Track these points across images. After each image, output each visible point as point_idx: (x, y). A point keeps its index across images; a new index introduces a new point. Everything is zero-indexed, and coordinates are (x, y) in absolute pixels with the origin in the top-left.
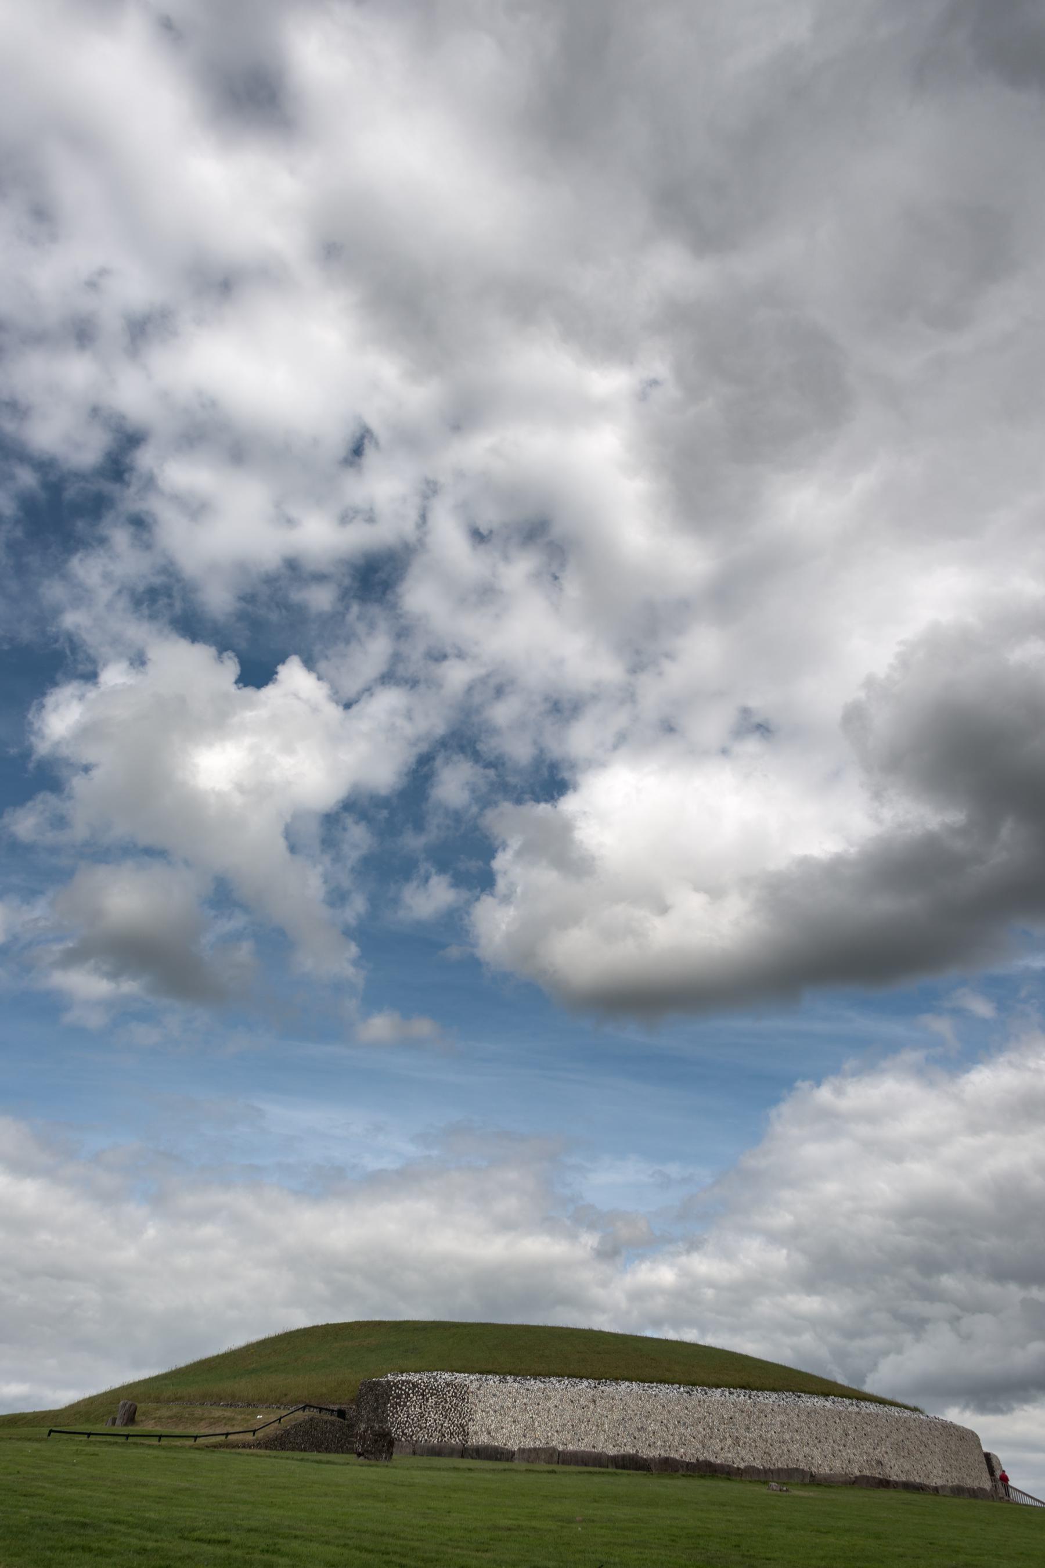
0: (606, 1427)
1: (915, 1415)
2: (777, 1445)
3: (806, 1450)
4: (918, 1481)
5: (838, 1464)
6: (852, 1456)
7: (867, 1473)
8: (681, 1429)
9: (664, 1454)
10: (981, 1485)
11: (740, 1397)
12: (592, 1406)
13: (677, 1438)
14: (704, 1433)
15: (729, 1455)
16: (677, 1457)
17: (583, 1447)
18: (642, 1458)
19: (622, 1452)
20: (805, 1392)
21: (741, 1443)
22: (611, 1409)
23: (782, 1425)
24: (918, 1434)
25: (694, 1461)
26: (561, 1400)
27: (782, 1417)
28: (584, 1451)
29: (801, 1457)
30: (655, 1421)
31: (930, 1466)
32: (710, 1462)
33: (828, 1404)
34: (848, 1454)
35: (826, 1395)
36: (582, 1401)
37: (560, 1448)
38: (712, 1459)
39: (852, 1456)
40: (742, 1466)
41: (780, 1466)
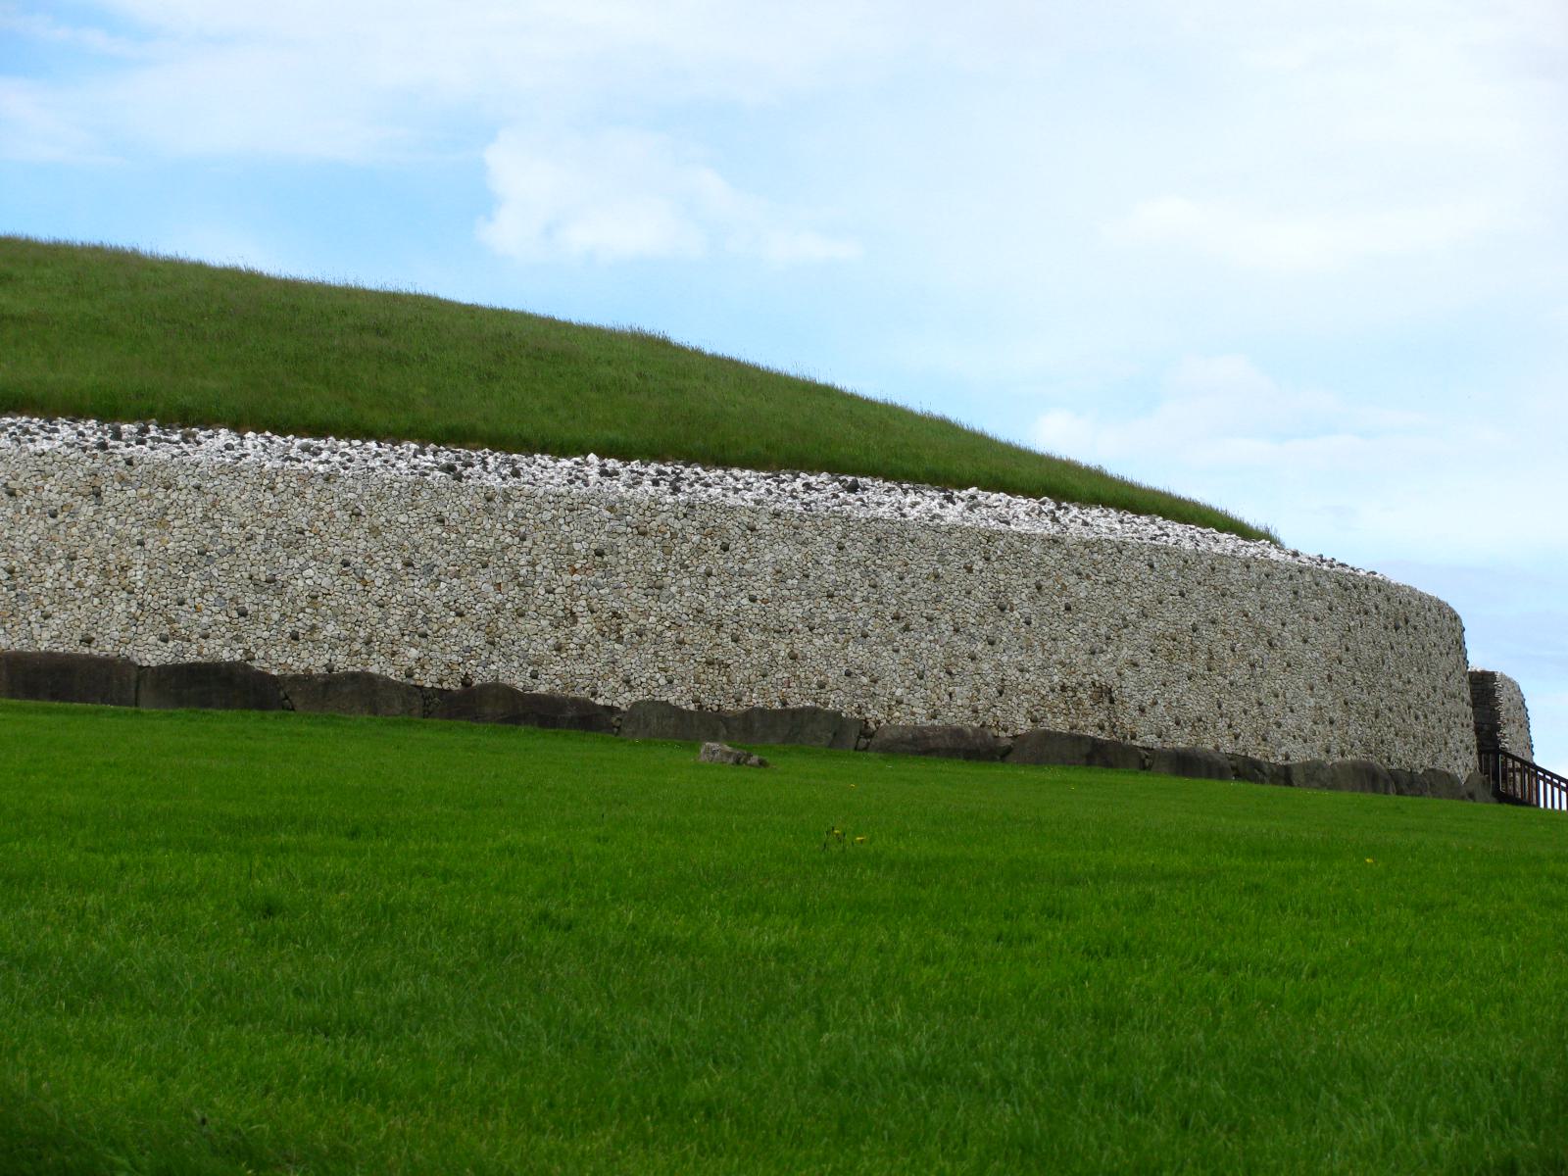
0: (137, 575)
1: (1253, 549)
3: (857, 653)
4: (1228, 747)
5: (962, 693)
6: (1012, 673)
7: (1059, 724)
8: (417, 587)
9: (342, 662)
10: (1440, 765)
11: (638, 484)
12: (87, 510)
13: (397, 614)
16: (391, 673)
18: (263, 677)
19: (190, 657)
20: (874, 473)
22: (160, 520)
23: (780, 576)
24: (1247, 606)
25: (453, 685)
27: (784, 551)
28: (50, 655)
29: (833, 676)
30: (321, 558)
31: (1273, 706)
32: (510, 692)
33: (953, 513)
34: (998, 666)
35: (946, 481)
36: (51, 493)
38: (519, 682)
39: (1012, 673)
40: (624, 700)
41: (758, 702)
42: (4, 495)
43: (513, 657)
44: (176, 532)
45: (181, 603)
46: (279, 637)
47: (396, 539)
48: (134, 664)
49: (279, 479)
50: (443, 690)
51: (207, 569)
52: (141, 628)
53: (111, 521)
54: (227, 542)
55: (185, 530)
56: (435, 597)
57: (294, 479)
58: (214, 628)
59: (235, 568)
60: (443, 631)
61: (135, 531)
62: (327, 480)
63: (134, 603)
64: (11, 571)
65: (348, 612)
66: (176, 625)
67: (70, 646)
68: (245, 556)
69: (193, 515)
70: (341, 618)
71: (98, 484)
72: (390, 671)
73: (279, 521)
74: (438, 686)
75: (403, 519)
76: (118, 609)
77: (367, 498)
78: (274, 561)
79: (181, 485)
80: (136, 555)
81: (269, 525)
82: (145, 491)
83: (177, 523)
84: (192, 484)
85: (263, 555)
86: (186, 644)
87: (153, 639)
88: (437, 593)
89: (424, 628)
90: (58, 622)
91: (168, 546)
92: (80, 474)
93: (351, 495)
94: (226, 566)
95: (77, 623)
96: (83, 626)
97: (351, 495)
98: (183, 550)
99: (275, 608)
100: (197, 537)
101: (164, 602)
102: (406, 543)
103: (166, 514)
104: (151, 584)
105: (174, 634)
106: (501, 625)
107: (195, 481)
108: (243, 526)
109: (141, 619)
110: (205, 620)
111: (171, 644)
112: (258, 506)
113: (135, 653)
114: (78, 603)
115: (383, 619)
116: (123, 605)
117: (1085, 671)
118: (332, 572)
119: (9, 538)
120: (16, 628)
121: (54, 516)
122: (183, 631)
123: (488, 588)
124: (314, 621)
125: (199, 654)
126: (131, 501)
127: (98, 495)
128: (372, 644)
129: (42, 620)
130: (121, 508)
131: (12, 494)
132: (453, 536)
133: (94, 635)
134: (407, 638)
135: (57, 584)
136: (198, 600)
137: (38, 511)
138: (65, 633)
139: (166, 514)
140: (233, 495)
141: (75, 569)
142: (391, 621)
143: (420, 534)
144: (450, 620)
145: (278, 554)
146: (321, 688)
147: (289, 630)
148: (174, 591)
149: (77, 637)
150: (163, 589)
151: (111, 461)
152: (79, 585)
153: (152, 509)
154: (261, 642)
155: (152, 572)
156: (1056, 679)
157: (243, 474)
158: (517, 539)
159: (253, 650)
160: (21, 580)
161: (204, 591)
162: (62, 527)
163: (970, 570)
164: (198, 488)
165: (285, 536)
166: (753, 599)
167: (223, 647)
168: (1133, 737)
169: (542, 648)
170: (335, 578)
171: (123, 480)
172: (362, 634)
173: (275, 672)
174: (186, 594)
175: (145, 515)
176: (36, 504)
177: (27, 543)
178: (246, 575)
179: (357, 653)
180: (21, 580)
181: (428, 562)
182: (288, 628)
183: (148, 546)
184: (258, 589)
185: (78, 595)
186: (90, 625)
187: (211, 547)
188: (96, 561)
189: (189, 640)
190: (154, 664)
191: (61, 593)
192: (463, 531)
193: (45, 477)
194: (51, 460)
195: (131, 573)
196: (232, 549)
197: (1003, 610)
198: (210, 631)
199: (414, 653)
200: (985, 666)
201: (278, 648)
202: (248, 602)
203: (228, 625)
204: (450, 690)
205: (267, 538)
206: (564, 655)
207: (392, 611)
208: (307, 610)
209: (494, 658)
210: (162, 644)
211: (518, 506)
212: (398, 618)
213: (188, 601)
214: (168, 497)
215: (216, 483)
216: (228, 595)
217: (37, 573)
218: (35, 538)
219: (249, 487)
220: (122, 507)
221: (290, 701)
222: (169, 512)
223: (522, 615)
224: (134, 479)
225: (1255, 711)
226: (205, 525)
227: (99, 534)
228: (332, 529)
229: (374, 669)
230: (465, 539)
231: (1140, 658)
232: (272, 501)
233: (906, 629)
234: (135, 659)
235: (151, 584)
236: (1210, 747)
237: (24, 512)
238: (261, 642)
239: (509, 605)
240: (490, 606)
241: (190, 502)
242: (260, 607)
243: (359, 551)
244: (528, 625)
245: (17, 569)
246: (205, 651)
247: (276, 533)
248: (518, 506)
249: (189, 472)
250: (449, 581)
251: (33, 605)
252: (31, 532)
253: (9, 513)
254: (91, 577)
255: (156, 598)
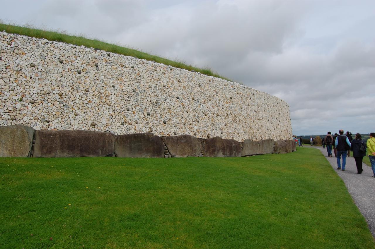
0: (112, 99)
2: (256, 121)
8: (195, 106)
9: (180, 133)
12: (93, 71)
13: (192, 115)
14: (213, 110)
15: (230, 131)
16: (191, 134)
17: (78, 124)
19: (134, 132)
21: (237, 119)
26: (42, 58)
28: (79, 132)
36: (79, 64)
37: (38, 127)
42: (58, 63)
43: (217, 128)
44: (126, 83)
45: (128, 110)
46: (160, 123)
47: (190, 91)
48: (113, 135)
49: (158, 68)
50: (203, 139)
51: (136, 97)
52: (114, 120)
53: (102, 77)
54: (143, 88)
55: (129, 83)
56: (200, 109)
57: (162, 68)
58: (140, 120)
59: (146, 98)
60: (202, 120)
61: (111, 81)
62: (171, 70)
63: (111, 110)
64: (61, 95)
65: (179, 114)
66: (127, 119)
67: (87, 128)
68: (149, 94)
69: (131, 77)
70: (177, 116)
71: (97, 62)
72: (191, 134)
73: (159, 82)
74: (202, 138)
75: (191, 84)
76: (105, 112)
77: (182, 77)
78: (157, 96)
79: (127, 66)
80: (112, 91)
81: (156, 83)
82: (115, 67)
83: (126, 80)
84: (131, 66)
85: (154, 93)
86: (130, 126)
87: (119, 124)
88: (200, 108)
89: (198, 120)
90: (81, 117)
91: (123, 88)
92: (90, 57)
93: (178, 76)
94: (143, 97)
95: (89, 118)
96: (92, 119)
97: (178, 76)
98: (128, 90)
99: (158, 113)
100: (133, 86)
101: (122, 110)
102: (192, 92)
103: (122, 76)
104: (118, 103)
105: (126, 122)
106: (214, 119)
107: (131, 65)
108: (147, 83)
109: (114, 116)
110: (136, 117)
111: (125, 126)
112: (152, 76)
113: (112, 130)
114: (90, 109)
115: (188, 116)
116: (107, 111)
118: (174, 101)
119: (60, 81)
120: (63, 120)
121: (79, 73)
122: (129, 121)
123: (211, 107)
124: (170, 117)
125: (135, 130)
126: (110, 70)
127: (97, 66)
128: (186, 125)
129: (75, 116)
130: (106, 72)
131: (61, 62)
132: (203, 91)
133: (96, 123)
134: (194, 123)
135: (81, 101)
136: (134, 109)
137: (73, 70)
138: (84, 122)
139: (122, 76)
140: (144, 71)
141: (88, 95)
142: (190, 117)
143: (195, 90)
144: (204, 117)
145: (159, 93)
146: (176, 141)
147: (163, 120)
148: (126, 105)
149: (89, 123)
150: (121, 105)
151: (102, 54)
152: (90, 102)
153: (117, 74)
154: (154, 125)
155: (117, 98)
157: (147, 65)
158: (216, 93)
159: (152, 127)
160: (65, 99)
161: (136, 106)
162: (83, 78)
164: (133, 67)
165: (160, 87)
166: (255, 112)
167: (143, 126)
169: (222, 125)
170: (175, 102)
171: (106, 62)
172: (183, 122)
173: (159, 136)
174: (130, 107)
175: (115, 76)
176: (72, 68)
177: (68, 84)
178: (149, 100)
179: (182, 128)
180: (65, 99)
181: (198, 98)
182: (162, 119)
183: (116, 88)
184: (153, 106)
185: (89, 106)
186: (95, 119)
187: (138, 90)
188: (97, 93)
189: (131, 124)
190: (119, 134)
191: (82, 105)
192: (205, 90)
193: (76, 57)
194: (78, 51)
195: (110, 98)
196: (145, 91)
198: (138, 121)
199: (196, 127)
201: (160, 127)
202: (150, 110)
203: (144, 119)
204: (205, 139)
205: (155, 87)
206: (227, 127)
207: (190, 114)
208: (168, 113)
209: (214, 128)
210: (122, 126)
211: (215, 83)
212: (191, 116)
213: (131, 109)
214: (123, 70)
215: (139, 66)
216: (144, 108)
217: (72, 96)
218: (71, 81)
219: (149, 69)
220: (106, 71)
221: (167, 146)
222: (123, 75)
223: (218, 116)
224: (110, 62)
226: (136, 81)
227: (97, 82)
228: (173, 86)
229: (187, 133)
230: (205, 92)
232: (156, 75)
234: (112, 132)
235: (118, 103)
237: (67, 70)
238: (154, 125)
239: (215, 112)
240: (212, 113)
241: (130, 72)
242: (154, 112)
243: (181, 94)
244: (219, 118)
245: (64, 94)
246: (137, 129)
247: (158, 86)
248: (215, 83)
249: (130, 62)
250: (202, 105)
251: (71, 110)
252: (70, 79)
253: (60, 70)
254: (95, 99)
255: (119, 108)
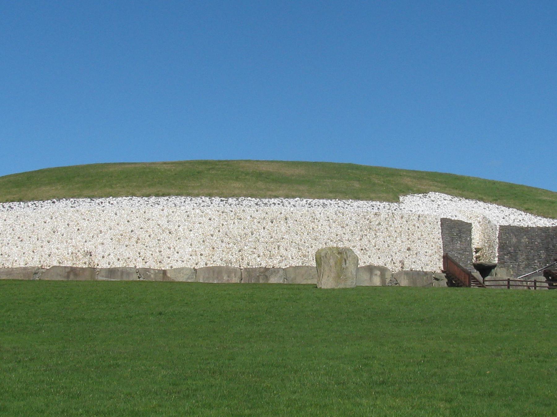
5: (36, 259)
117: (82, 247)
156: (70, 251)
163: (45, 222)
168: (98, 265)
197: (54, 232)
200: (45, 249)
225: (158, 254)
231: (105, 241)
233: (21, 241)
236: (132, 266)
